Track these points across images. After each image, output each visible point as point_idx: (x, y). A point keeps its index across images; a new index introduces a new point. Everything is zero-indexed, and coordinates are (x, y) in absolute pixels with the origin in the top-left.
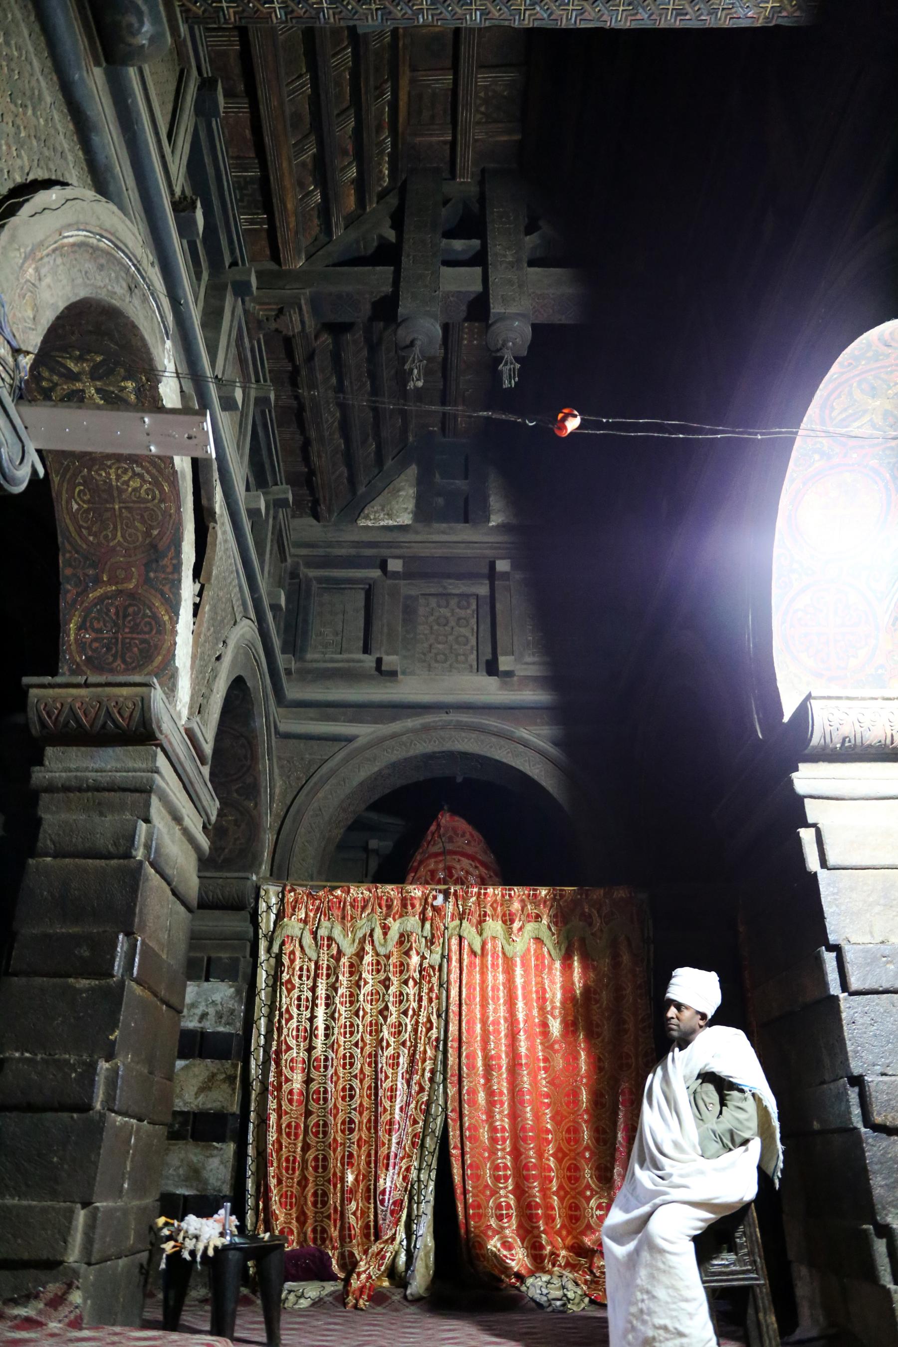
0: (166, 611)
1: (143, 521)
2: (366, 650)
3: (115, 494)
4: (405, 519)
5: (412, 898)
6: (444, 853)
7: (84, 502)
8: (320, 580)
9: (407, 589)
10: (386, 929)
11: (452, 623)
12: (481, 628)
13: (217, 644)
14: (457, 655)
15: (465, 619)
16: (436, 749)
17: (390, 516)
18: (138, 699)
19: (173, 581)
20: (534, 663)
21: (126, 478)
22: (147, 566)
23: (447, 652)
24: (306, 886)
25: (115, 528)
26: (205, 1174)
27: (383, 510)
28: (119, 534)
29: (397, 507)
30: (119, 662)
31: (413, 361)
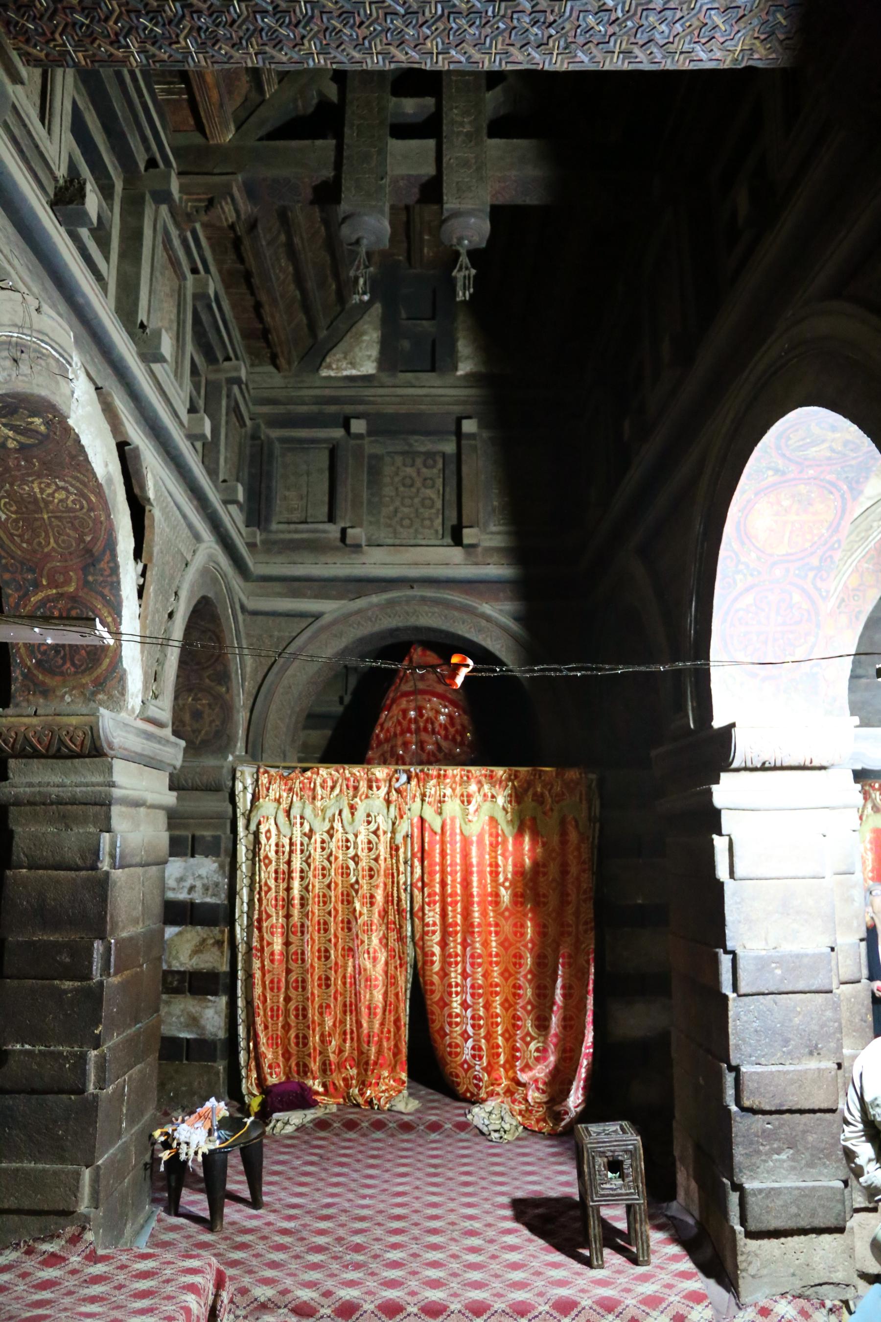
0: (109, 613)
1: (75, 529)
2: (331, 519)
3: (42, 505)
4: (369, 368)
5: (377, 780)
6: (416, 692)
7: (12, 512)
8: (283, 440)
9: (370, 447)
10: (352, 808)
11: (418, 484)
12: (448, 490)
13: (168, 600)
14: (423, 520)
15: (431, 479)
16: (400, 624)
17: (353, 365)
18: (87, 728)
19: (112, 583)
20: (498, 533)
21: (49, 491)
22: (85, 569)
23: (412, 515)
24: (278, 767)
25: (47, 536)
26: (203, 1022)
27: (345, 358)
28: (52, 541)
29: (360, 354)
30: (68, 665)
31: (358, 268)
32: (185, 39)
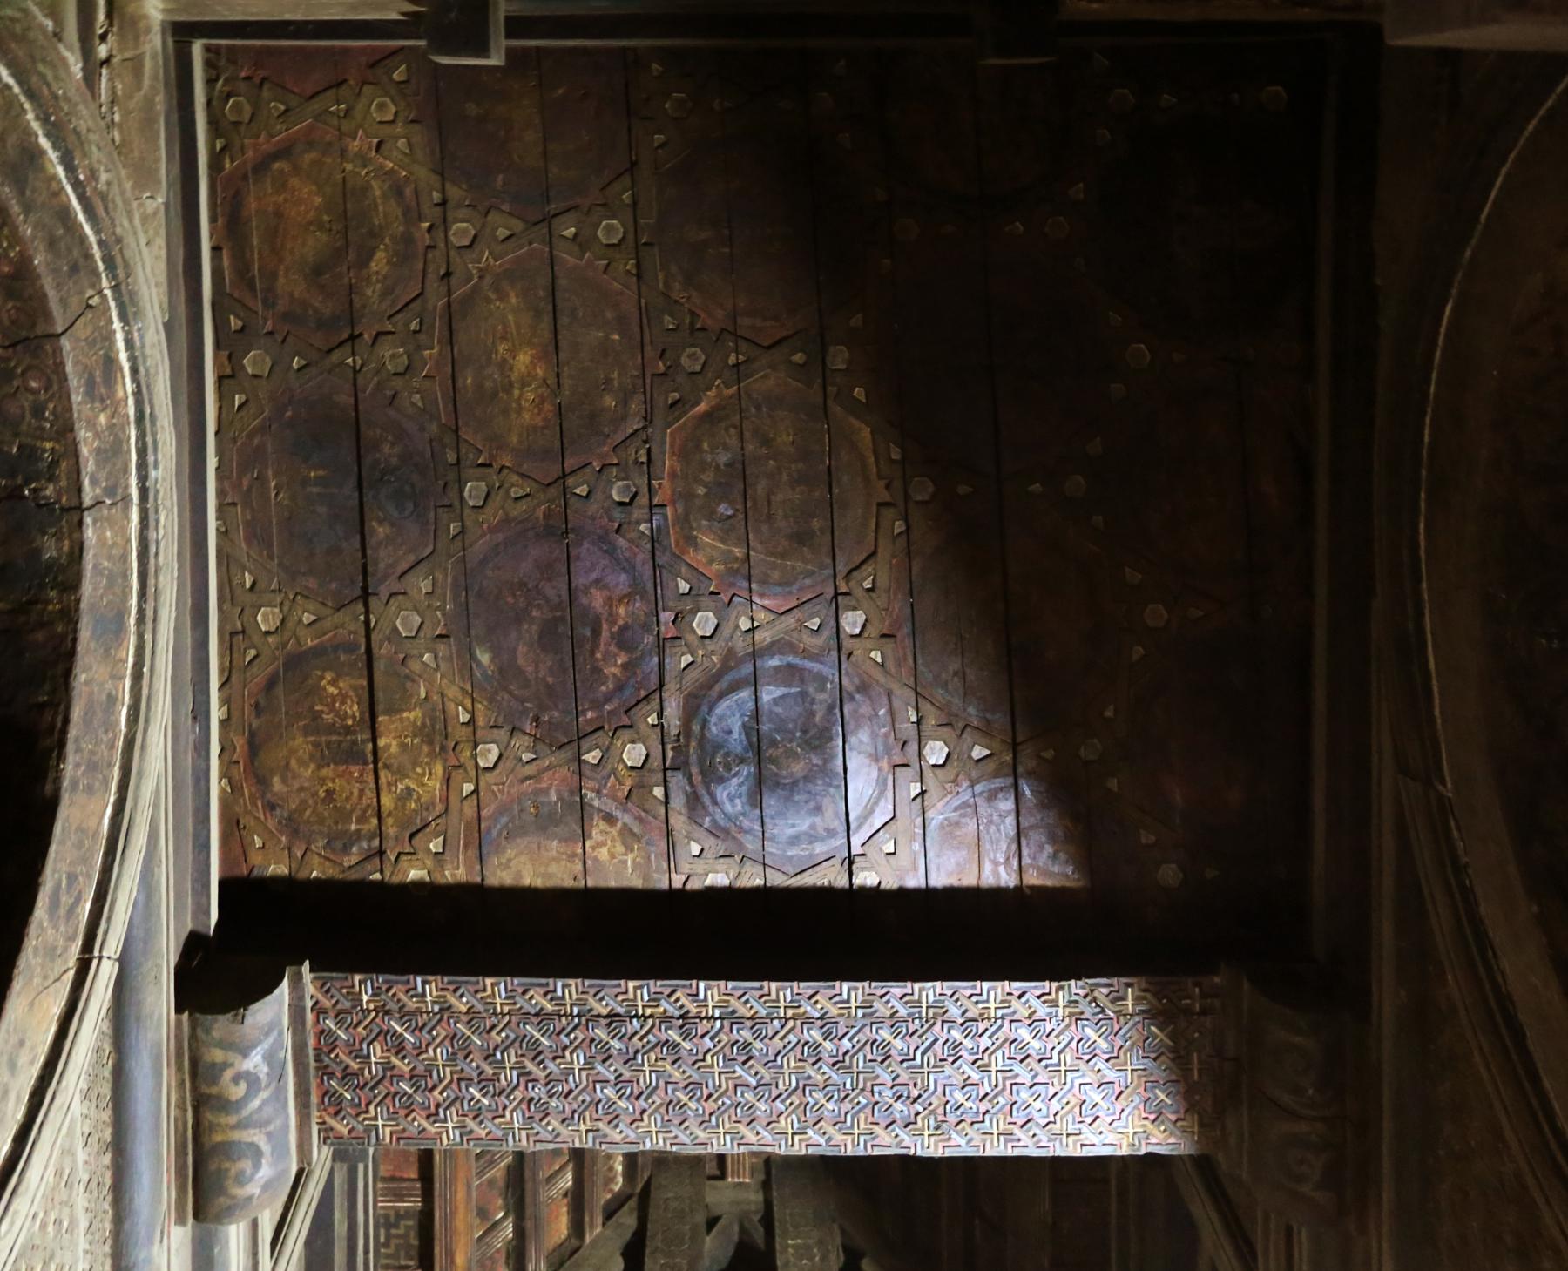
32: (512, 1112)
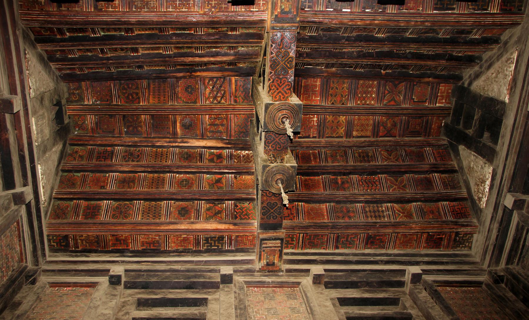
17: (483, 182)
